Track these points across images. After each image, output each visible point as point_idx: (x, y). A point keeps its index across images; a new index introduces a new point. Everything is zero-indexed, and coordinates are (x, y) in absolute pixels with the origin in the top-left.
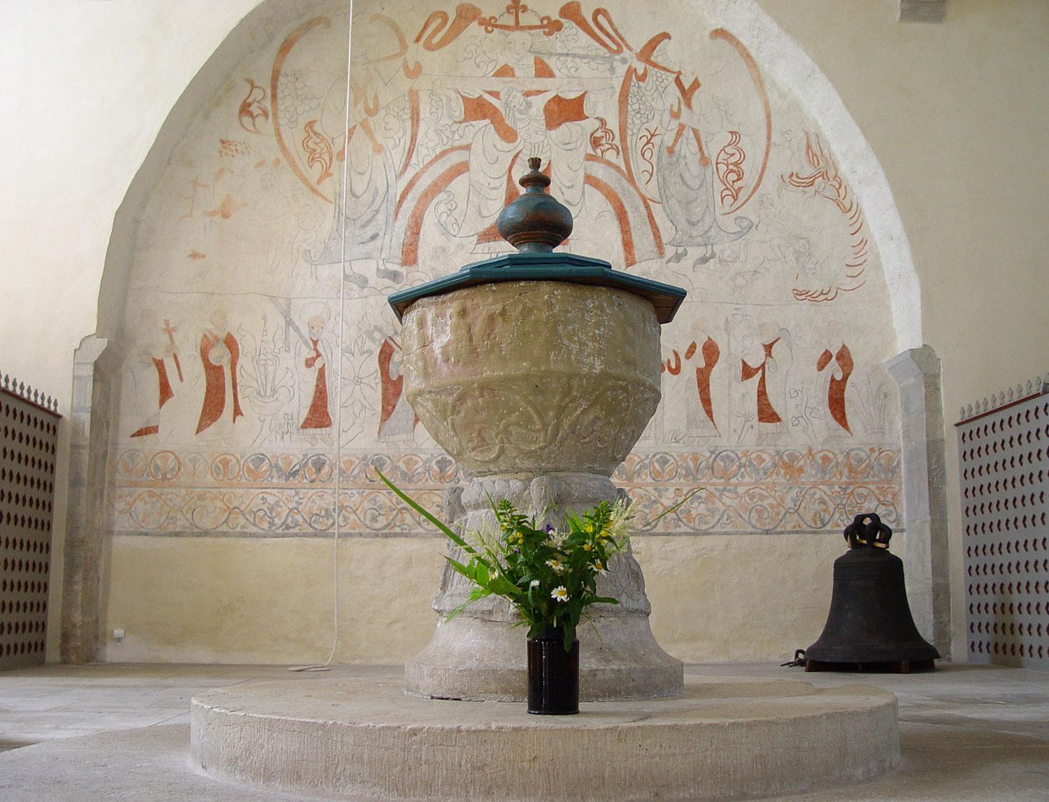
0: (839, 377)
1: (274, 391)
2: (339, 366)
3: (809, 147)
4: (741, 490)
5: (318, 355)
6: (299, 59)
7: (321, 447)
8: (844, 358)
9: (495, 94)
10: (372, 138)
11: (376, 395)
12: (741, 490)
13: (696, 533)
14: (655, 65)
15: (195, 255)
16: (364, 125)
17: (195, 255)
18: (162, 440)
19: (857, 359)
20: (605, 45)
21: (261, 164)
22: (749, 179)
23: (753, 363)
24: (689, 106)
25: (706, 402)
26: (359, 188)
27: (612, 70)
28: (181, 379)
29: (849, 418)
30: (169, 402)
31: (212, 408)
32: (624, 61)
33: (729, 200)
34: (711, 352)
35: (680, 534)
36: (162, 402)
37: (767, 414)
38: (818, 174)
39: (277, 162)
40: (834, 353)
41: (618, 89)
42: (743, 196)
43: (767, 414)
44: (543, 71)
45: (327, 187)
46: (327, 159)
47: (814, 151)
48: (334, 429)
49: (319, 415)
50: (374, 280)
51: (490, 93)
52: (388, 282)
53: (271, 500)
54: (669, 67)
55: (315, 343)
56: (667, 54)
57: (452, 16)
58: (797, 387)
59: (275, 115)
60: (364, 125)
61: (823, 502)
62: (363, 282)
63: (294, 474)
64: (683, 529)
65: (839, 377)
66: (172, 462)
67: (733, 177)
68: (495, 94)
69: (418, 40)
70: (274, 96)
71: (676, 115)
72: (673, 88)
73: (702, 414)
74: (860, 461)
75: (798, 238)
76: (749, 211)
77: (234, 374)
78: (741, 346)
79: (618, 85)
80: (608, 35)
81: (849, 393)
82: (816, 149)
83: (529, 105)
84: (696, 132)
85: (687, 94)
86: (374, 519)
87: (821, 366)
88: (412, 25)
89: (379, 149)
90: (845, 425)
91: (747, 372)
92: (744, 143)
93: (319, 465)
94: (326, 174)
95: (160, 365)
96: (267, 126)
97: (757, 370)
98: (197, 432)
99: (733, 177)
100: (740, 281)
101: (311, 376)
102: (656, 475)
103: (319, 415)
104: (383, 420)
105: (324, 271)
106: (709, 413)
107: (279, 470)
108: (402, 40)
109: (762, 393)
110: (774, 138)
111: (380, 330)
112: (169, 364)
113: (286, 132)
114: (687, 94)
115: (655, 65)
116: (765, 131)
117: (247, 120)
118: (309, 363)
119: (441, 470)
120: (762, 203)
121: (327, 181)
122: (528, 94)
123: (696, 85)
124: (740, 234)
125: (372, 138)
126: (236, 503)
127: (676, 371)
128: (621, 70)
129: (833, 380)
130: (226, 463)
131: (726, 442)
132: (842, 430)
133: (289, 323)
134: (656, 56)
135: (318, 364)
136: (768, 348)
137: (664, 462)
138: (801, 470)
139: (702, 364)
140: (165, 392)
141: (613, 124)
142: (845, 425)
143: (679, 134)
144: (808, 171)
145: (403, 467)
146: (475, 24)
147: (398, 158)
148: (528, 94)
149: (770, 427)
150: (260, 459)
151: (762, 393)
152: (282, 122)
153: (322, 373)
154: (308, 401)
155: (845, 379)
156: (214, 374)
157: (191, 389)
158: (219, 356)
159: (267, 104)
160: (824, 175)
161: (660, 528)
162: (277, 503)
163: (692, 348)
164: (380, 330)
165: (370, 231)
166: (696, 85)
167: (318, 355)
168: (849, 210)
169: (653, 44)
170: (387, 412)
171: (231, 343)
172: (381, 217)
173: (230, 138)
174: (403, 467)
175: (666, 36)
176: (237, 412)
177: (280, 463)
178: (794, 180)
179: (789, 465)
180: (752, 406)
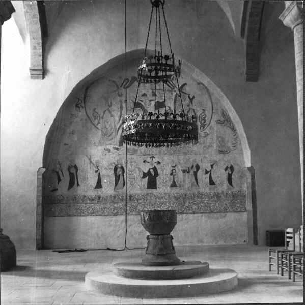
0: (230, 173)
1: (87, 179)
2: (103, 172)
3: (223, 113)
4: (205, 202)
5: (98, 170)
6: (89, 93)
7: (100, 193)
8: (232, 168)
9: (142, 101)
10: (110, 113)
11: (113, 179)
12: (205, 202)
13: (194, 213)
14: (183, 92)
15: (65, 144)
16: (109, 110)
17: (65, 144)
18: (58, 193)
19: (236, 168)
20: (170, 87)
21: (82, 120)
22: (207, 122)
23: (208, 170)
24: (192, 103)
25: (196, 180)
26: (108, 126)
27: (172, 94)
28: (63, 176)
29: (233, 183)
30: (60, 182)
31: (71, 184)
32: (175, 91)
33: (202, 128)
34: (198, 167)
35: (190, 213)
36: (58, 183)
37: (212, 182)
38: (226, 120)
39: (86, 120)
40: (229, 166)
41: (173, 99)
42: (206, 127)
43: (212, 182)
44: (155, 95)
45: (99, 126)
46: (99, 118)
47: (224, 114)
48: (103, 189)
49: (99, 185)
50: (112, 150)
51: (140, 101)
52: (116, 151)
53: (88, 207)
54: (187, 92)
55: (98, 167)
56: (187, 89)
57: (130, 80)
58: (220, 175)
59: (85, 107)
60: (109, 110)
61: (226, 205)
62: (109, 151)
63: (93, 200)
64: (191, 212)
65: (230, 173)
66: (61, 198)
67: (203, 121)
68: (142, 101)
69: (121, 87)
70: (85, 102)
71: (188, 106)
72: (188, 98)
73: (195, 183)
74: (236, 194)
75: (220, 137)
76: (207, 131)
77: (77, 176)
78: (206, 165)
79: (173, 97)
80: (171, 84)
81: (233, 177)
82: (225, 114)
83: (151, 104)
84: (193, 110)
85: (191, 100)
86: (114, 211)
87: (226, 169)
88: (119, 83)
89: (112, 116)
90: (232, 185)
91: (207, 172)
92: (206, 113)
93: (99, 198)
94: (99, 123)
95: (57, 173)
96: (83, 110)
97: (209, 172)
98: (69, 189)
99: (203, 121)
100: (205, 149)
101: (97, 175)
102: (184, 199)
103: (99, 185)
104: (115, 186)
105: (99, 148)
106: (197, 183)
107: (89, 199)
108: (117, 87)
109: (210, 177)
110: (214, 111)
111: (114, 163)
112: (60, 172)
113: (88, 112)
114: (191, 100)
115: (183, 92)
116: (211, 109)
117: (77, 108)
118: (96, 172)
119: (130, 198)
120: (210, 128)
121: (99, 124)
122: (150, 101)
123: (194, 97)
124: (205, 137)
125: (110, 113)
126: (78, 208)
127: (188, 172)
128: (174, 94)
129: (229, 174)
130: (75, 197)
131: (202, 190)
132: (231, 187)
133: (91, 162)
134: (183, 90)
135: (98, 172)
136: (212, 166)
137: (186, 195)
138: (220, 197)
139: (195, 170)
140: (59, 180)
141: (172, 108)
142: (232, 185)
143: (189, 110)
144: (223, 119)
145: (120, 197)
146: (136, 82)
147: (117, 119)
148: (150, 101)
149: (213, 186)
150: (85, 196)
151: (210, 177)
152: (87, 109)
153: (99, 173)
154: (96, 181)
155: (232, 173)
156: (72, 175)
157: (66, 180)
158: (73, 171)
159: (83, 105)
160: (227, 121)
161: (185, 212)
162: (89, 208)
163: (193, 166)
164: (114, 163)
165: (110, 138)
166: (194, 97)
167: (98, 170)
168: (233, 129)
169: (183, 86)
170: (116, 183)
171: (76, 167)
172: (113, 134)
173: (73, 113)
174: (120, 197)
175: (185, 84)
176: (78, 184)
177: (90, 197)
178: (218, 122)
179: (218, 196)
180: (208, 180)
